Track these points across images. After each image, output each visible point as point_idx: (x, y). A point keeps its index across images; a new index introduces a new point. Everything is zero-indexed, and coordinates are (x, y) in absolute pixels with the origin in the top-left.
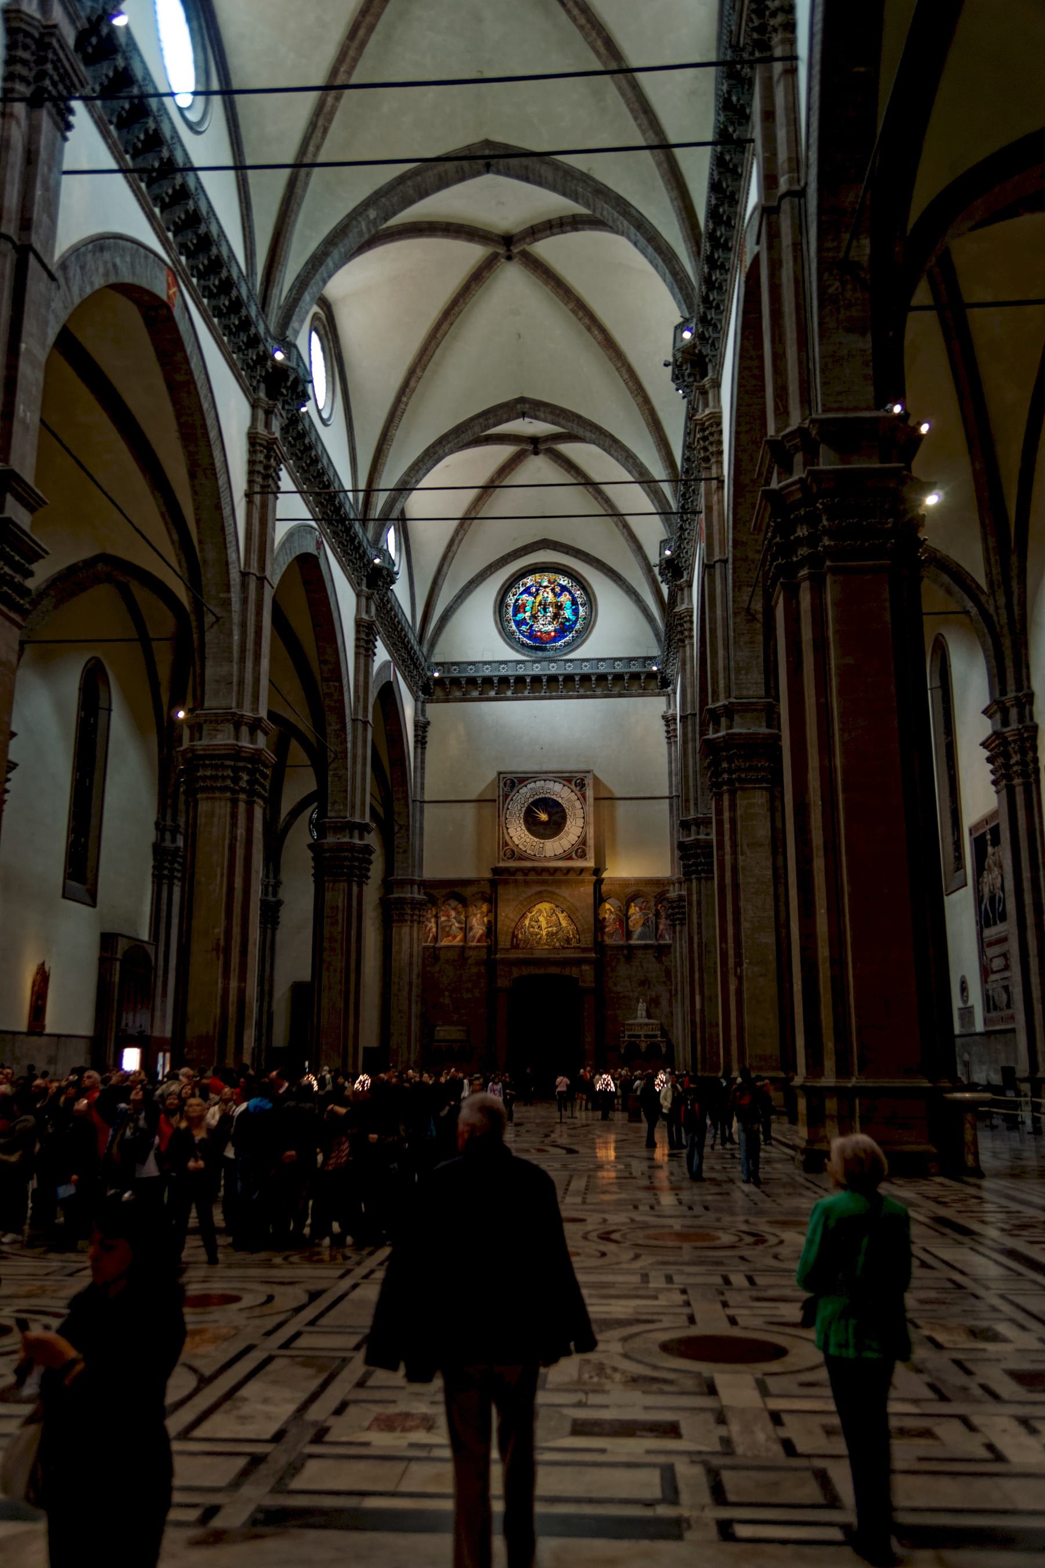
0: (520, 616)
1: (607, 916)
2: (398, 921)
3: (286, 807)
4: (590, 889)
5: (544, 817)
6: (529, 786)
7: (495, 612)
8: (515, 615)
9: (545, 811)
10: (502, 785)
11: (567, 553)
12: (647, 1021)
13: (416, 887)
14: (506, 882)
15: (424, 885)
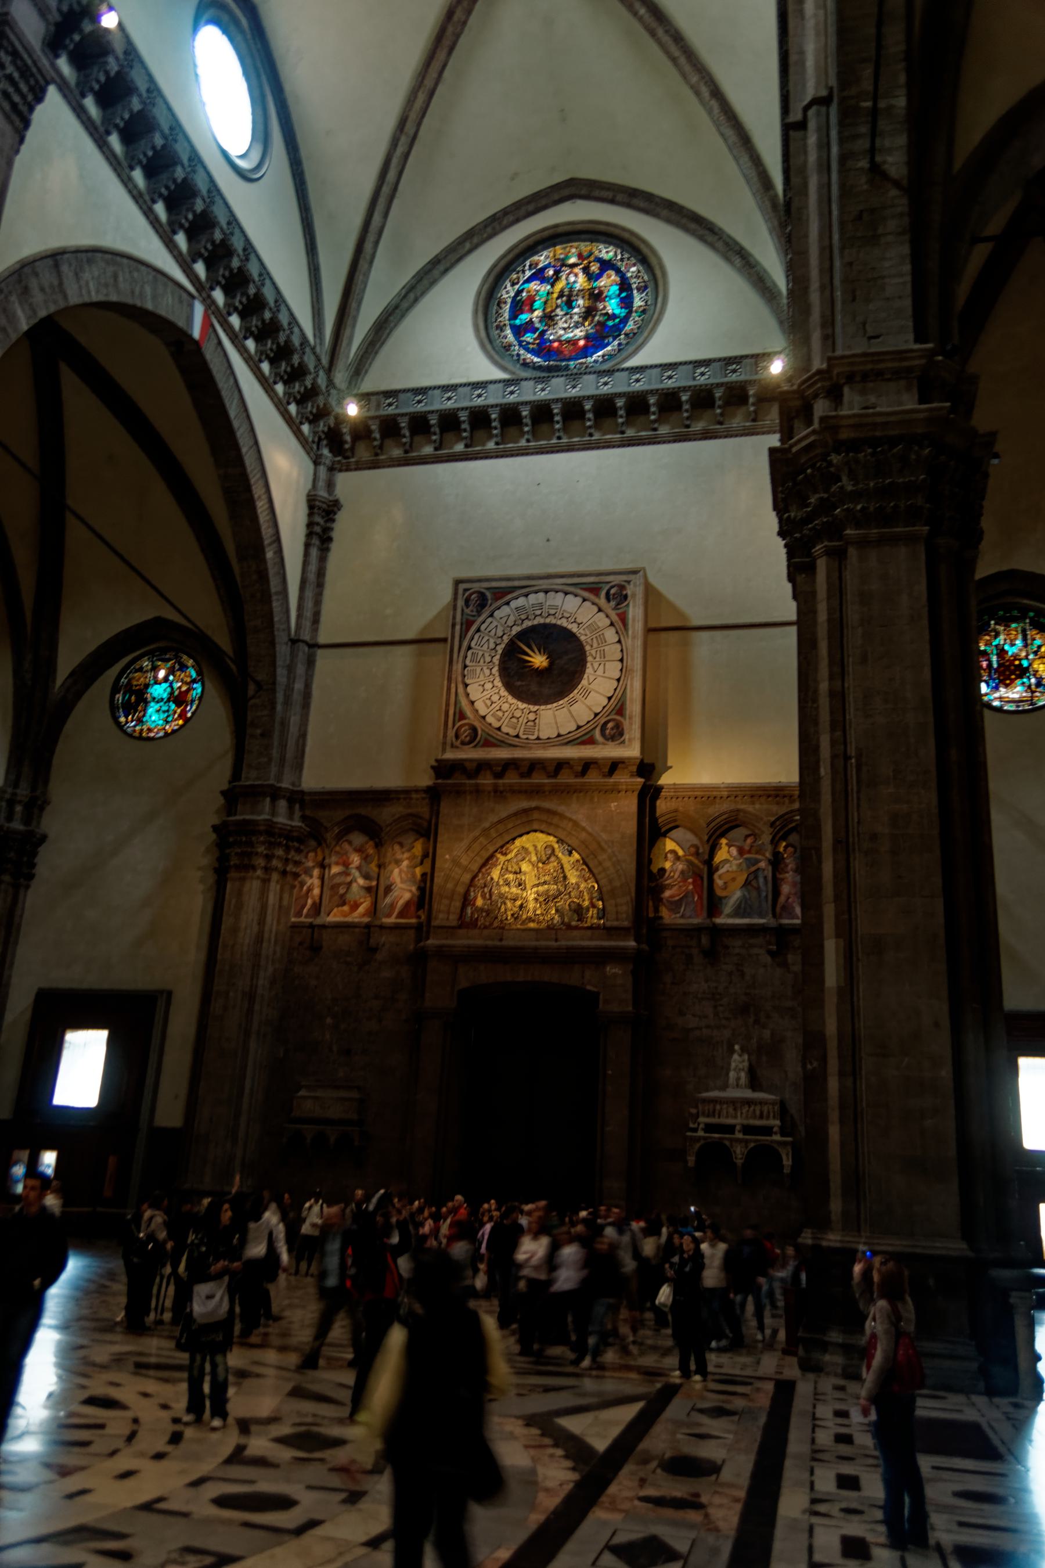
0: (524, 317)
1: (668, 865)
2: (238, 868)
3: (67, 661)
4: (629, 805)
5: (539, 660)
6: (514, 604)
7: (476, 312)
8: (514, 316)
9: (543, 649)
10: (460, 603)
11: (612, 201)
12: (749, 1094)
13: (282, 804)
14: (458, 792)
15: (297, 798)
